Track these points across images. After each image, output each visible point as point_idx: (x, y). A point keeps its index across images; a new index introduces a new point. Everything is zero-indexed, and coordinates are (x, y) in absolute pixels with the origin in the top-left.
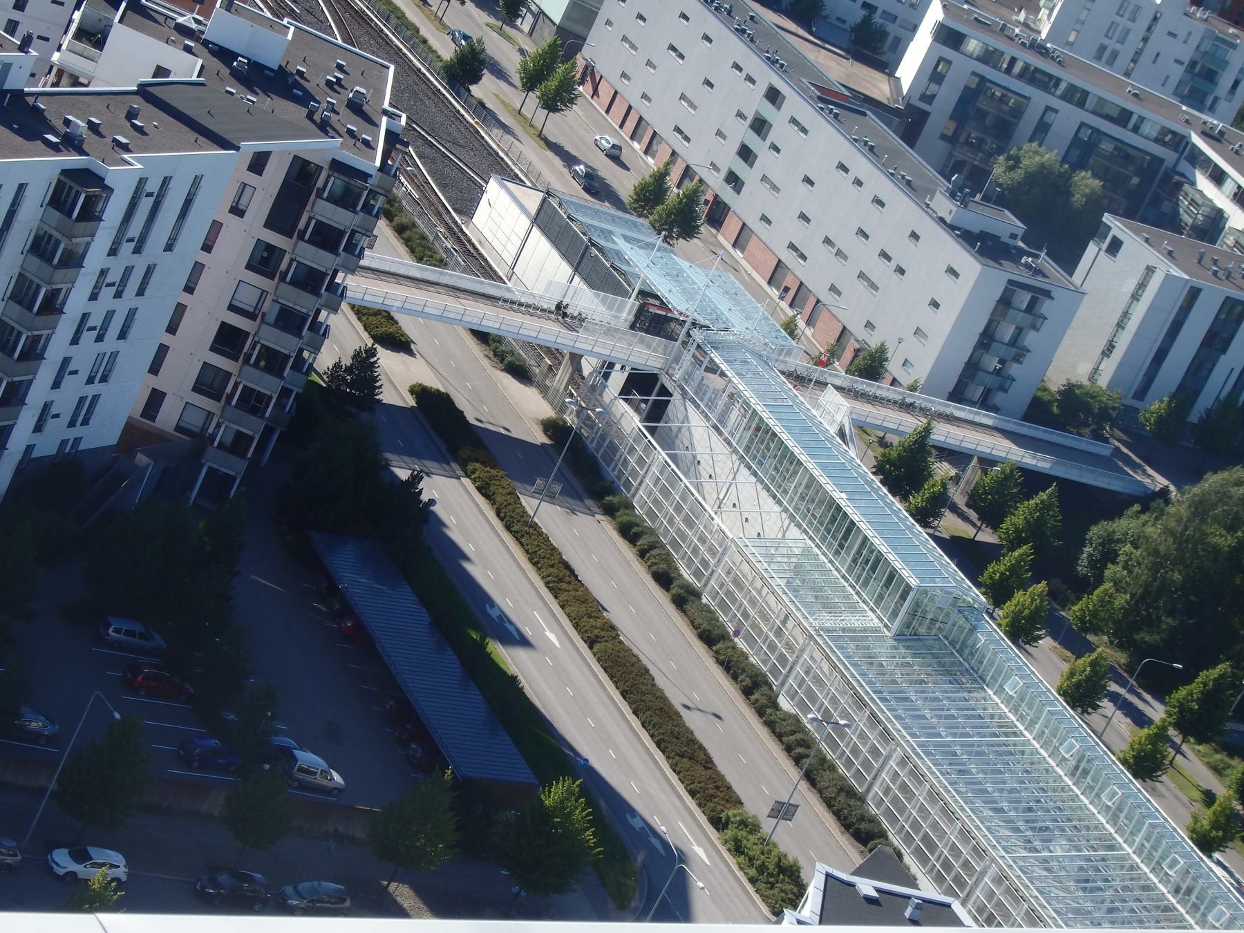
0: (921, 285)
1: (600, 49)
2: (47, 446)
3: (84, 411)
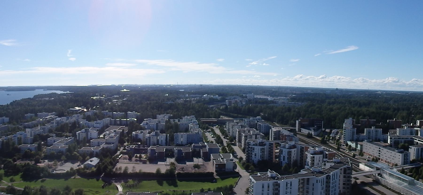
0: (397, 157)
1: (364, 150)
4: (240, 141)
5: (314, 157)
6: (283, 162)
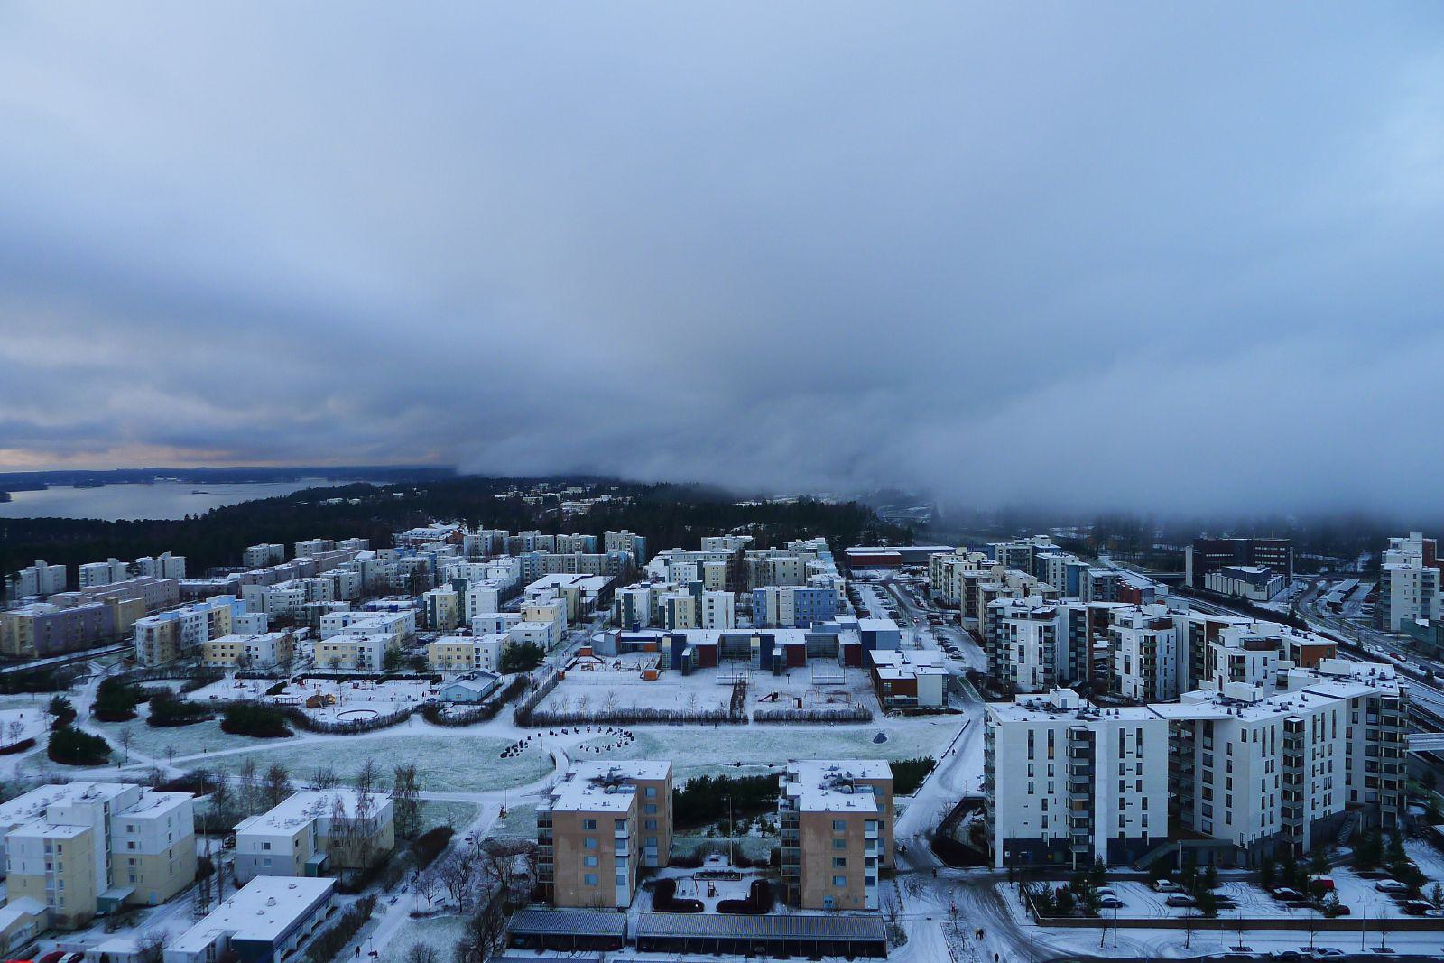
2: (1319, 814)
3: (1328, 800)
4: (972, 612)
6: (1125, 678)
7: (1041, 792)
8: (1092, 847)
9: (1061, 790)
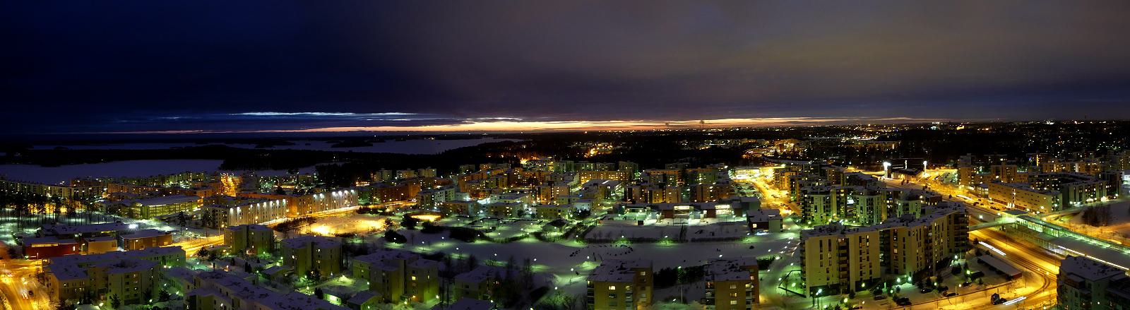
3: (941, 254)
5: (907, 205)
7: (826, 265)
8: (849, 286)
9: (835, 266)
